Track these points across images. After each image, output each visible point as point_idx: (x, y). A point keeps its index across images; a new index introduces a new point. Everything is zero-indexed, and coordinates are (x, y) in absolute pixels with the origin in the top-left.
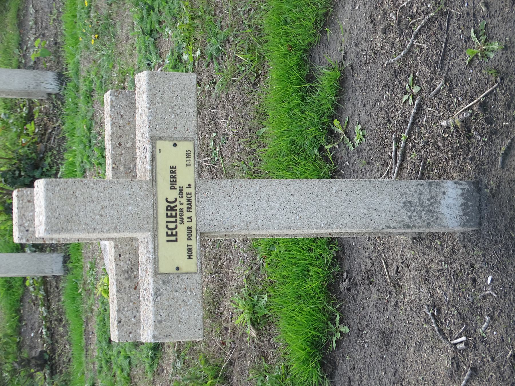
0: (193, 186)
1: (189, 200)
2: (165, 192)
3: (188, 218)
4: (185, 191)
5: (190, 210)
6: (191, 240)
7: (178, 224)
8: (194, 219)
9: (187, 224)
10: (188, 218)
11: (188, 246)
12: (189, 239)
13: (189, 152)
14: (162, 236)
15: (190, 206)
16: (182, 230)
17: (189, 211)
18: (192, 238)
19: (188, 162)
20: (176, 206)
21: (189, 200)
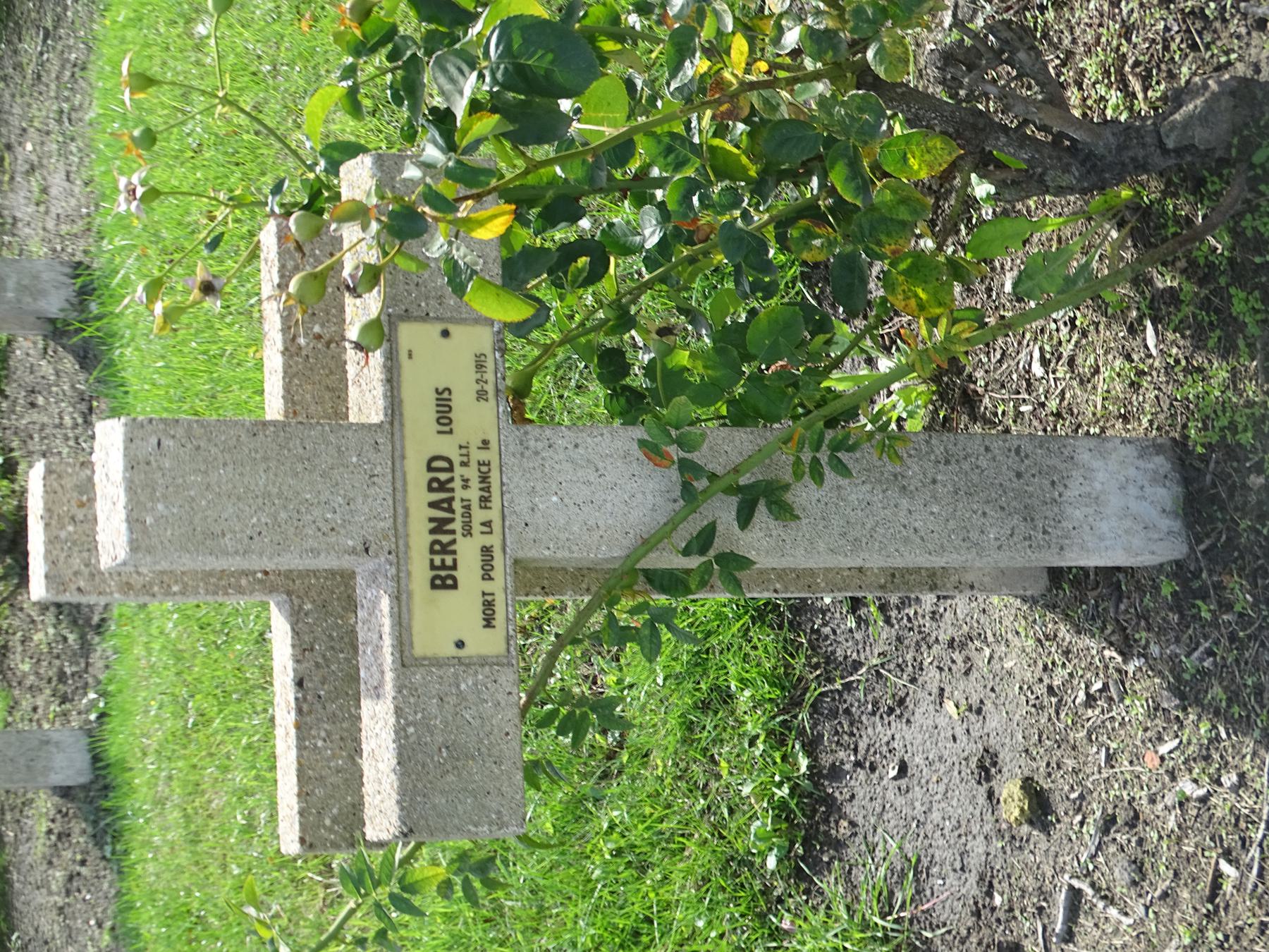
1: (484, 478)
3: (483, 524)
4: (477, 455)
6: (491, 579)
7: (458, 536)
8: (497, 526)
9: (478, 540)
10: (483, 524)
11: (484, 594)
12: (487, 577)
14: (420, 572)
15: (486, 494)
17: (486, 508)
18: (492, 574)
20: (451, 480)
21: (484, 478)
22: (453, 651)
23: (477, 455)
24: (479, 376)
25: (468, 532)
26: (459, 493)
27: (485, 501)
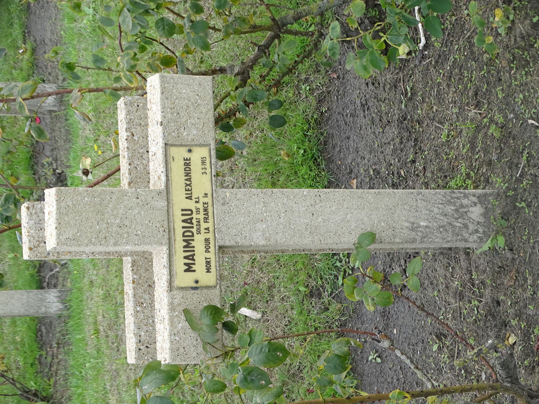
0: (209, 195)
1: (206, 210)
2: (180, 201)
3: (205, 229)
4: (202, 200)
5: (208, 221)
6: (209, 252)
8: (211, 229)
10: (205, 229)
11: (206, 258)
12: (207, 251)
13: (204, 159)
15: (207, 217)
16: (198, 242)
17: (206, 222)
19: (203, 171)
21: (206, 210)
22: (194, 285)
23: (202, 200)
24: (203, 166)
25: (199, 232)
26: (194, 216)
27: (206, 220)
